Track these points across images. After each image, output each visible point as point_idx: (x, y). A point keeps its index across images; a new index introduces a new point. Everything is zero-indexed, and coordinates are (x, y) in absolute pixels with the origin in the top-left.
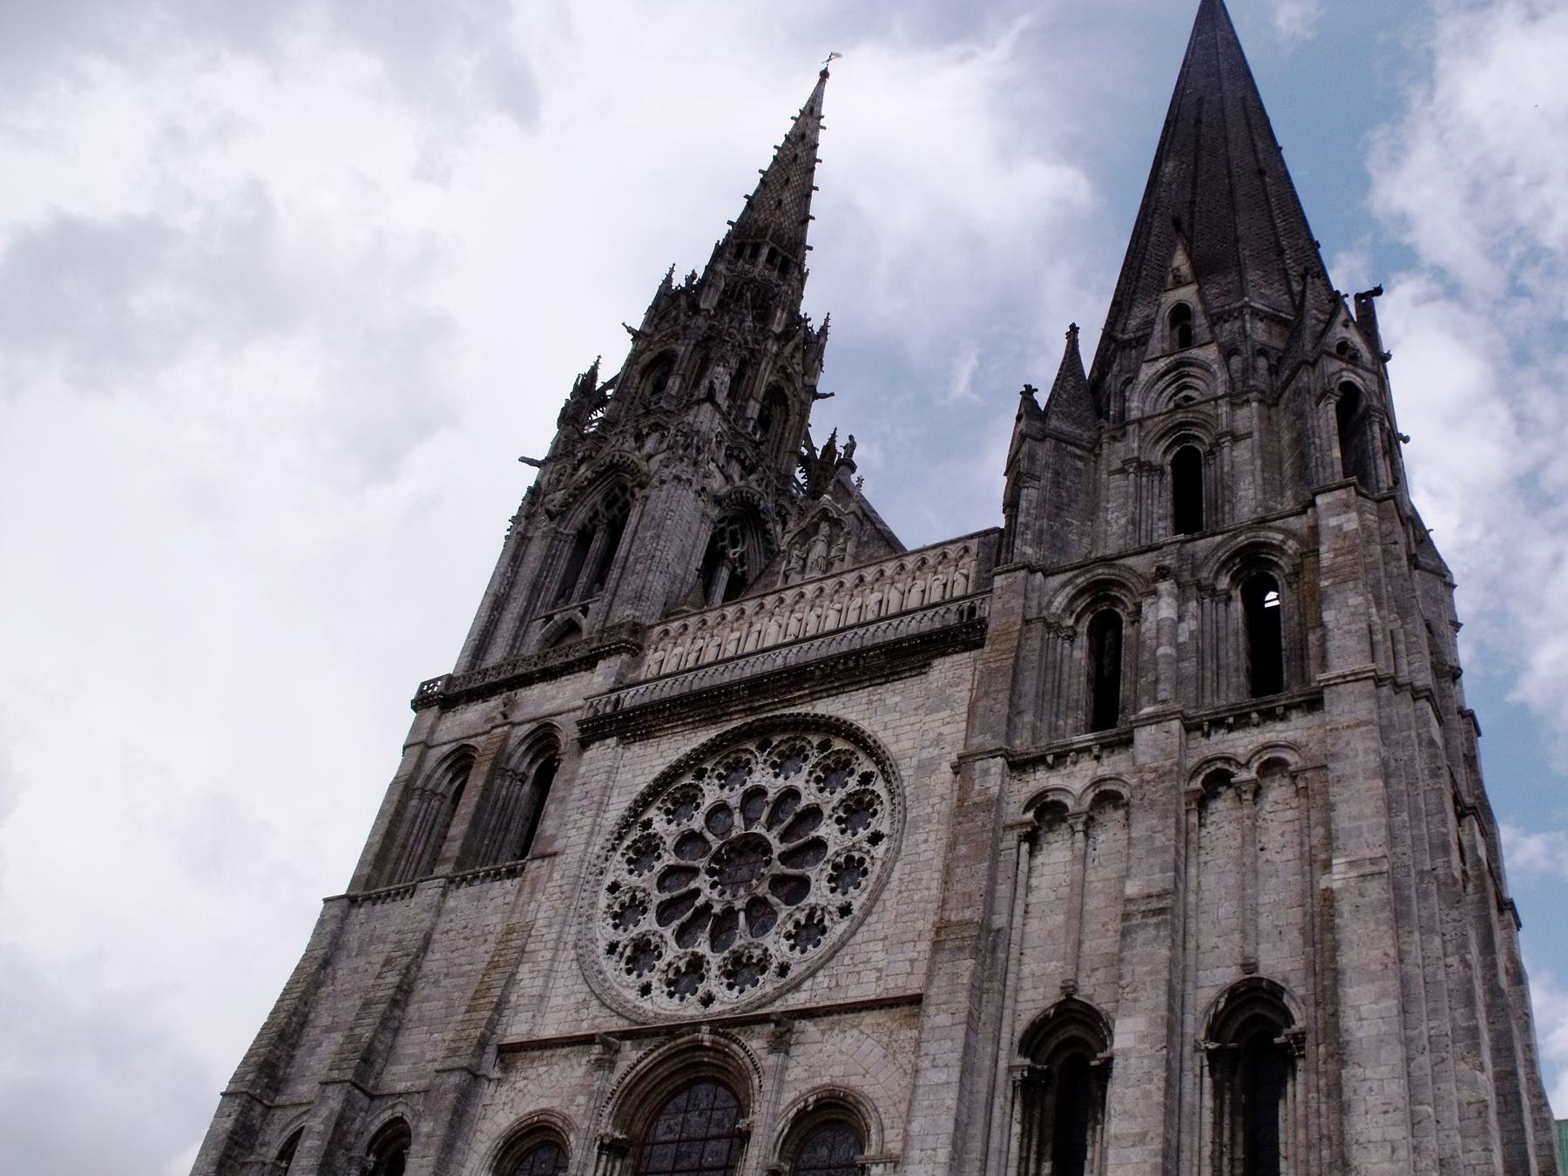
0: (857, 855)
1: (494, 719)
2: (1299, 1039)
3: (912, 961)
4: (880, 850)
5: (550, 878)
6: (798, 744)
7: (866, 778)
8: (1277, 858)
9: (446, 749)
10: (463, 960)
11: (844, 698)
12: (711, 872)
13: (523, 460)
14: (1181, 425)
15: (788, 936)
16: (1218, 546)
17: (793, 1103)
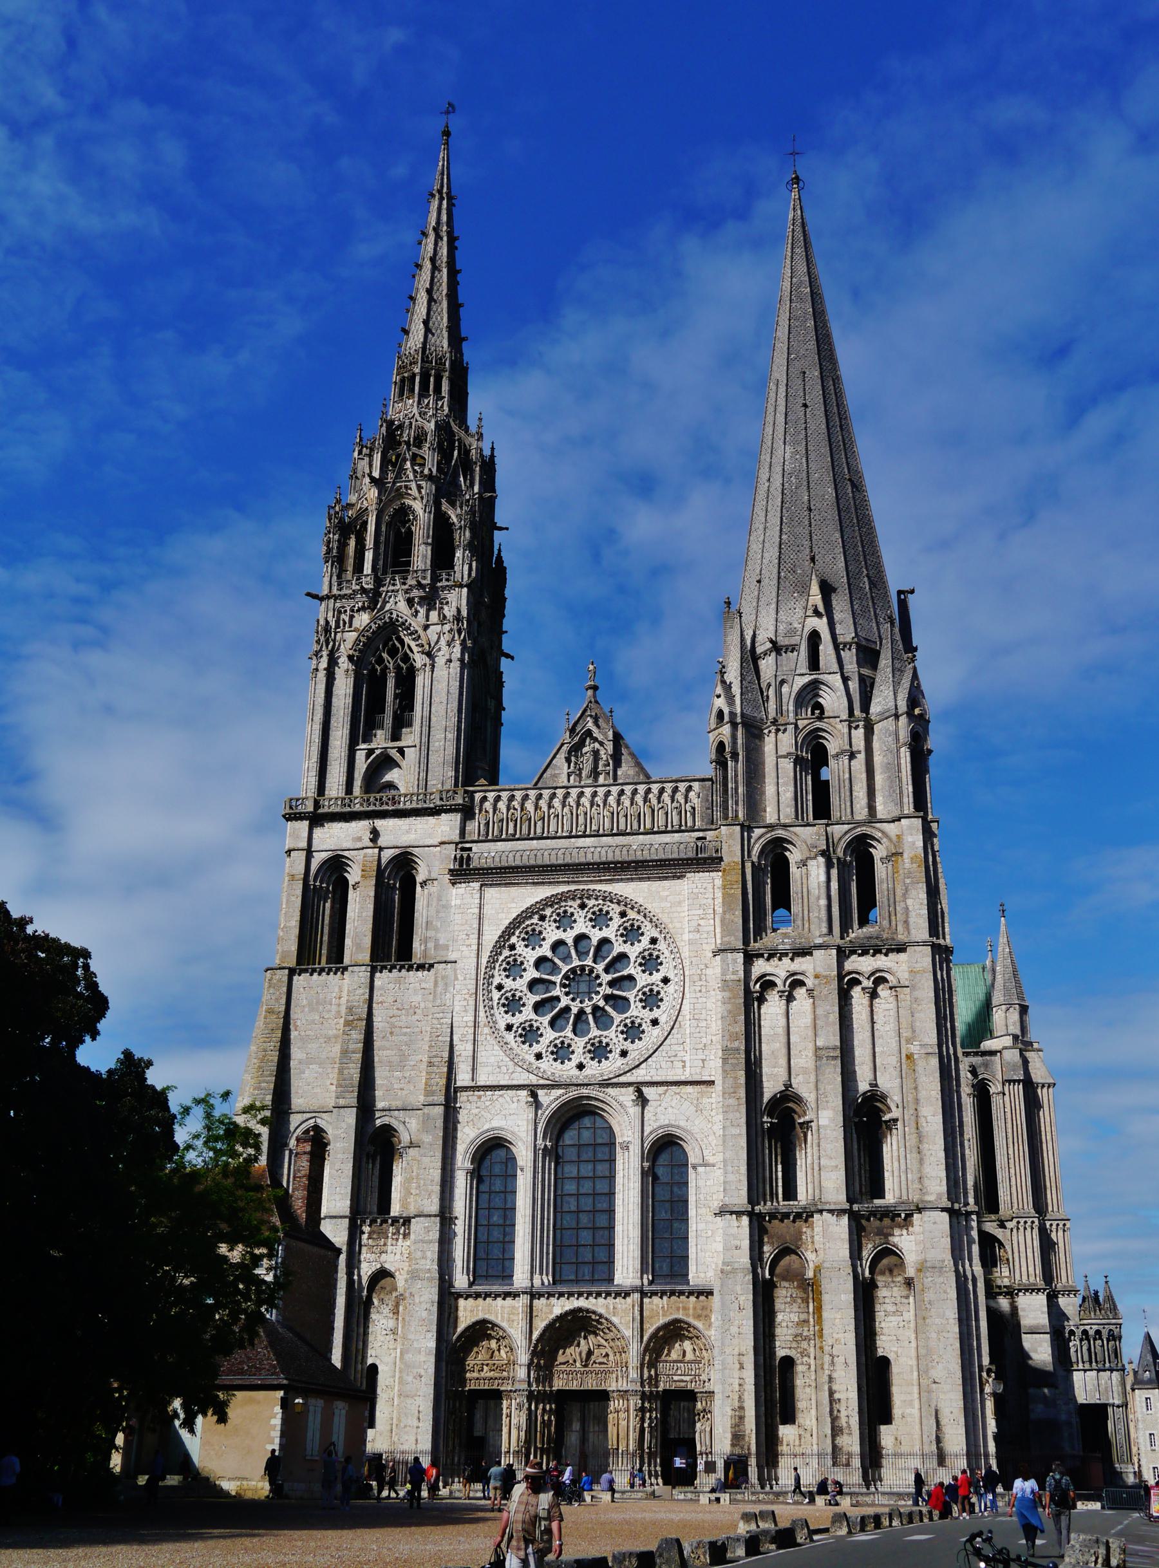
0: (656, 989)
1: (360, 839)
2: (896, 1120)
3: (703, 1061)
4: (671, 988)
5: (456, 979)
6: (605, 909)
7: (654, 941)
8: (882, 1029)
9: (324, 856)
10: (401, 1024)
11: (633, 885)
12: (564, 986)
13: (308, 594)
14: (819, 730)
15: (622, 1032)
16: (846, 833)
17: (651, 1133)
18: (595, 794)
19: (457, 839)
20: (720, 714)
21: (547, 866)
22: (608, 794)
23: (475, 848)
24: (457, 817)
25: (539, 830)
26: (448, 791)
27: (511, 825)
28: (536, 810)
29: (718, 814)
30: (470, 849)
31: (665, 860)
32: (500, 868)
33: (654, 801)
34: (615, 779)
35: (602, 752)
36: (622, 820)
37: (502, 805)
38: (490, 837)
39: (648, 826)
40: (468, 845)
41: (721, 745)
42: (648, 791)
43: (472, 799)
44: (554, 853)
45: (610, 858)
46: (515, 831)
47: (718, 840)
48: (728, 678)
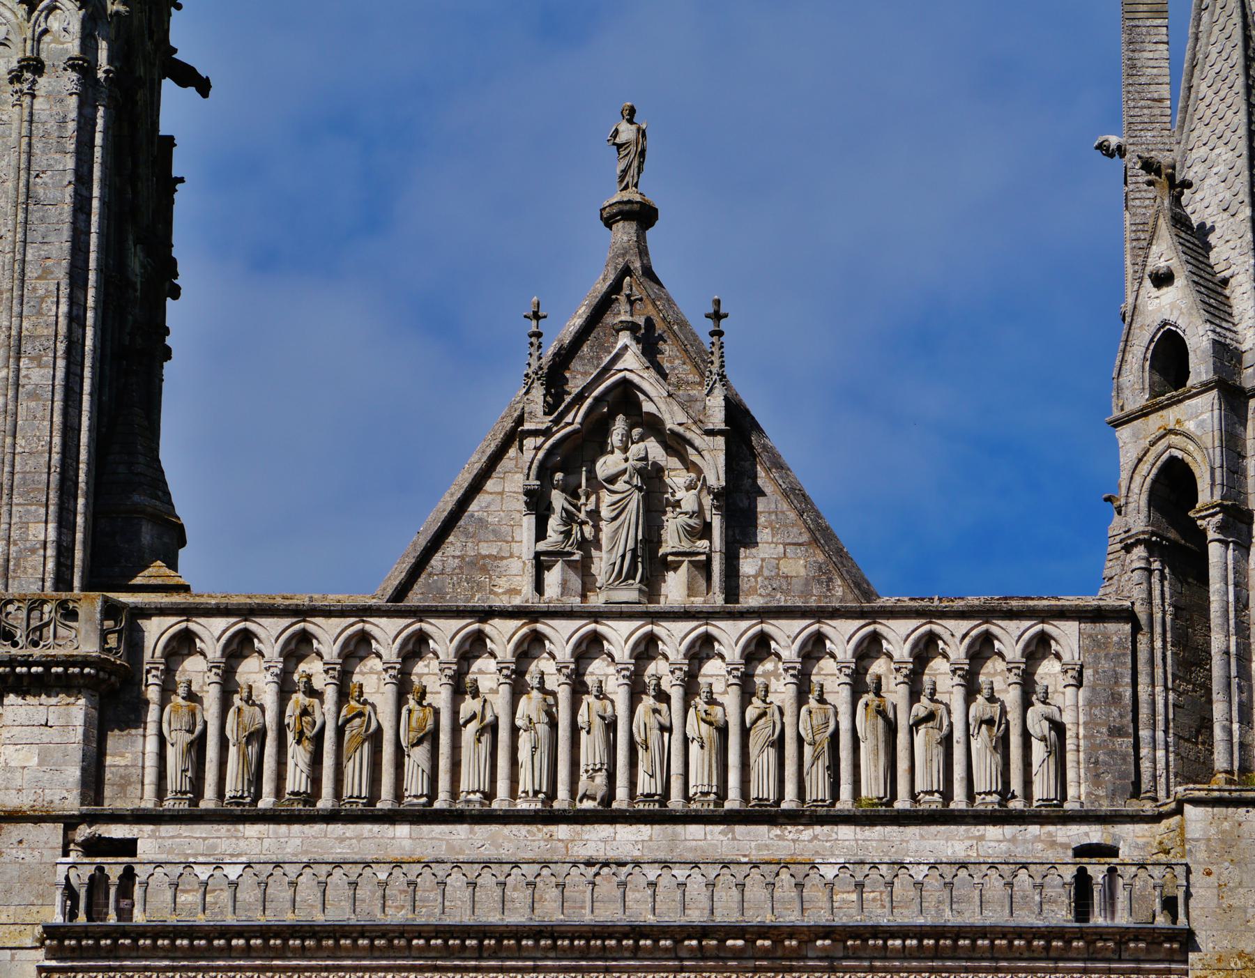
18: (647, 649)
19: (72, 803)
20: (1169, 354)
21: (463, 932)
22: (702, 649)
23: (151, 843)
24: (72, 714)
25: (415, 784)
26: (36, 604)
27: (298, 756)
28: (400, 700)
29: (1157, 758)
30: (128, 847)
31: (958, 932)
32: (265, 932)
33: (896, 693)
34: (732, 592)
35: (677, 478)
36: (763, 760)
37: (257, 675)
38: (209, 801)
39: (872, 787)
40: (118, 831)
41: (1173, 483)
42: (870, 647)
43: (134, 641)
44: (487, 879)
45: (727, 914)
46: (316, 780)
47: (1170, 858)
48: (1199, 207)
